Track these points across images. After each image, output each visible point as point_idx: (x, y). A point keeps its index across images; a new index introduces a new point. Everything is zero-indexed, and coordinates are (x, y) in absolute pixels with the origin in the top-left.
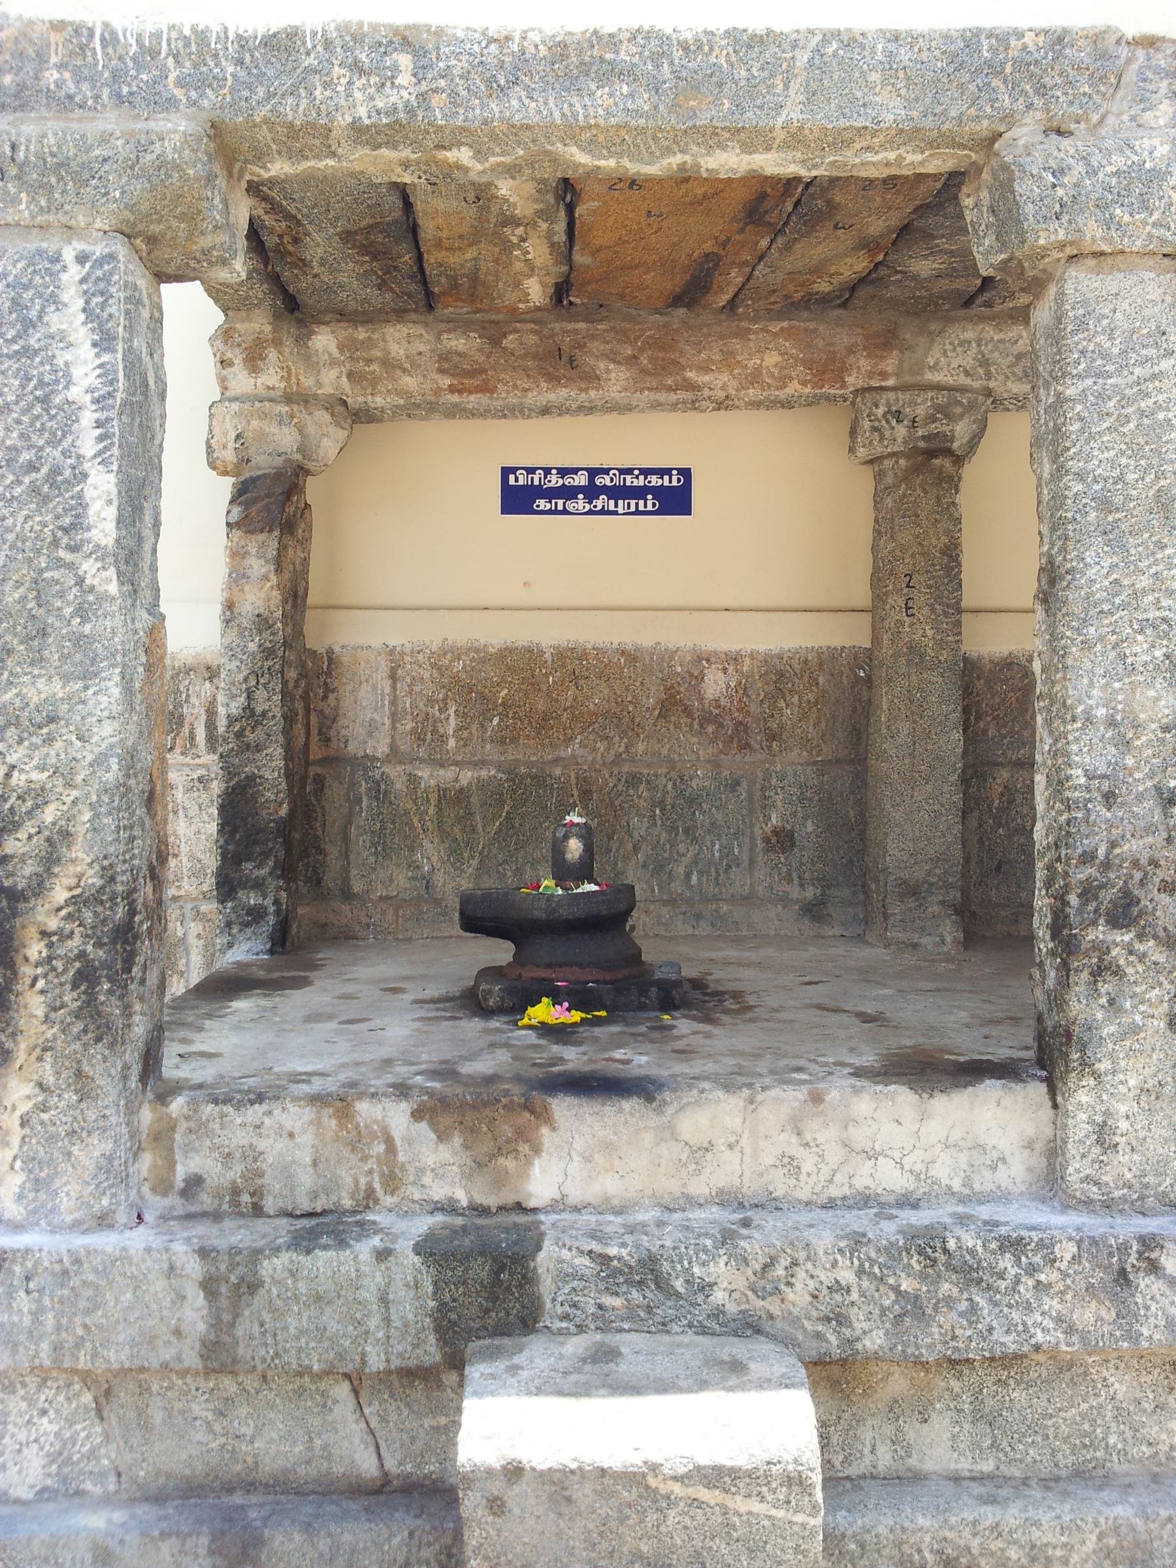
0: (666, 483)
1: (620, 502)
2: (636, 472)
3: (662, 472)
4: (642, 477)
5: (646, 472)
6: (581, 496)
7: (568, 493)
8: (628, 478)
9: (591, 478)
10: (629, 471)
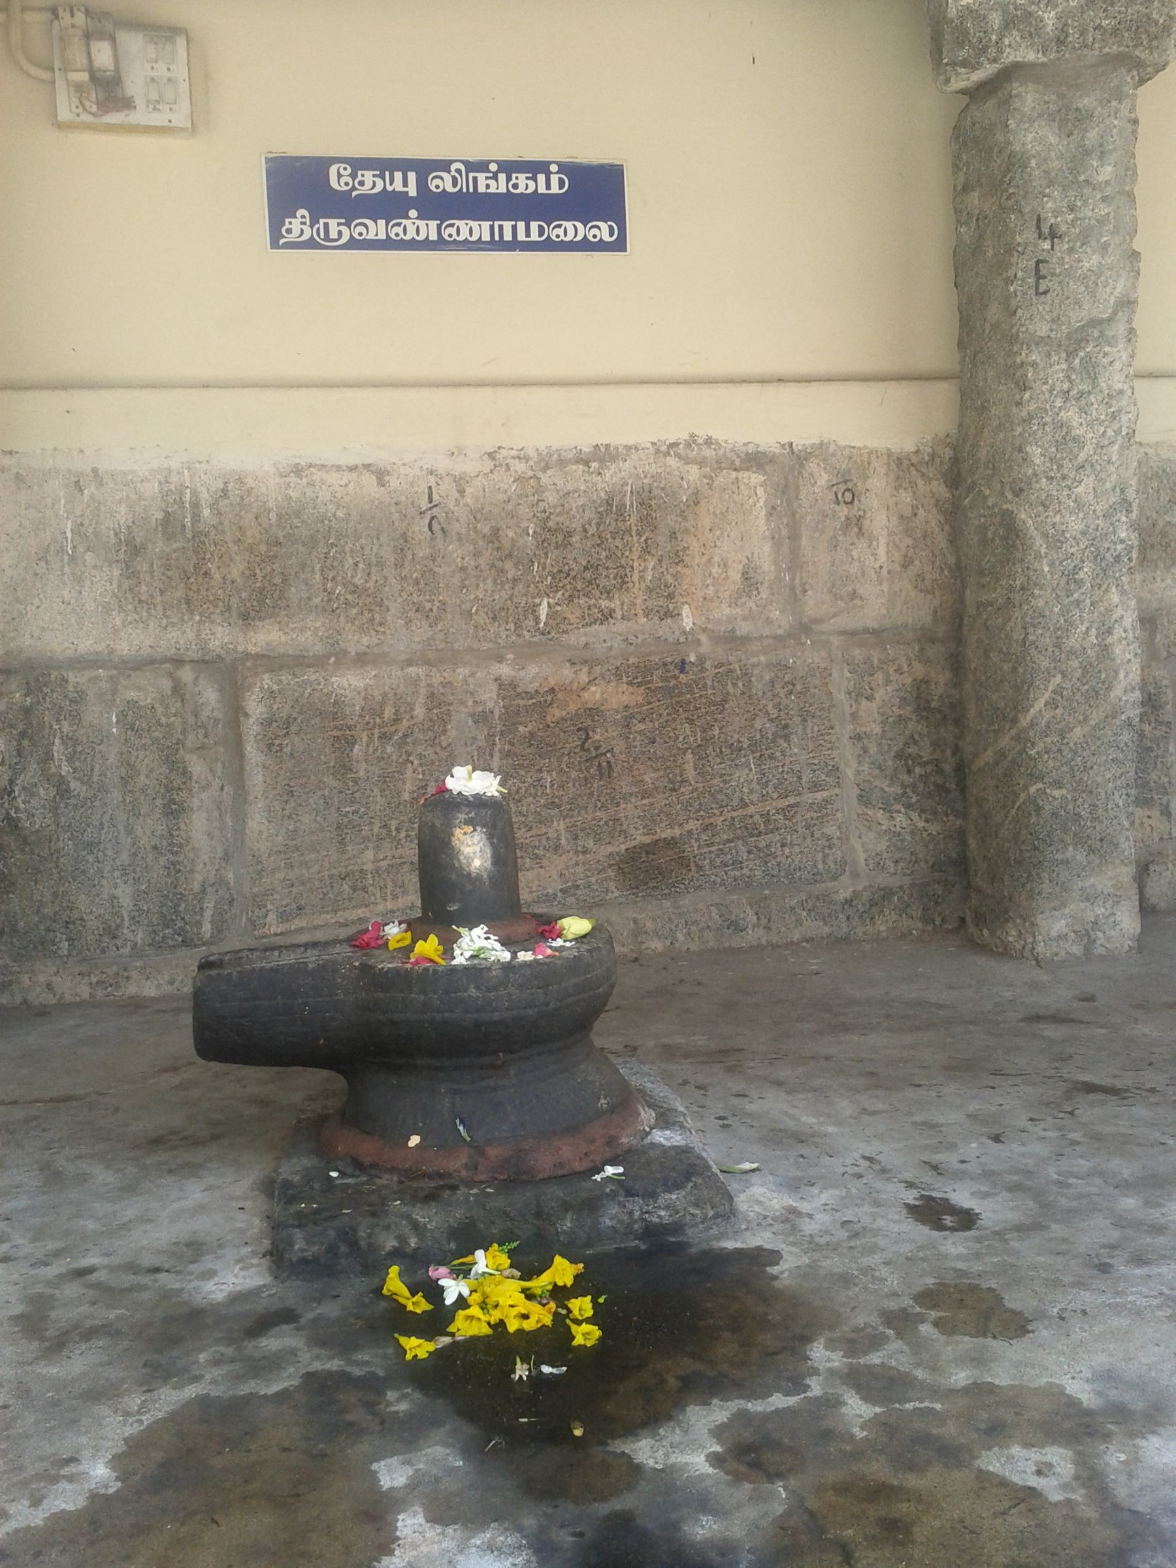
0: (542, 189)
1: (534, 226)
2: (493, 167)
3: (535, 168)
4: (502, 177)
5: (509, 168)
6: (413, 213)
7: (389, 206)
8: (481, 177)
9: (422, 184)
10: (482, 166)
